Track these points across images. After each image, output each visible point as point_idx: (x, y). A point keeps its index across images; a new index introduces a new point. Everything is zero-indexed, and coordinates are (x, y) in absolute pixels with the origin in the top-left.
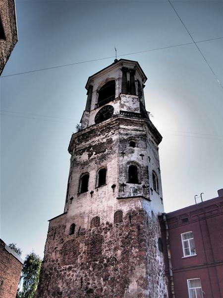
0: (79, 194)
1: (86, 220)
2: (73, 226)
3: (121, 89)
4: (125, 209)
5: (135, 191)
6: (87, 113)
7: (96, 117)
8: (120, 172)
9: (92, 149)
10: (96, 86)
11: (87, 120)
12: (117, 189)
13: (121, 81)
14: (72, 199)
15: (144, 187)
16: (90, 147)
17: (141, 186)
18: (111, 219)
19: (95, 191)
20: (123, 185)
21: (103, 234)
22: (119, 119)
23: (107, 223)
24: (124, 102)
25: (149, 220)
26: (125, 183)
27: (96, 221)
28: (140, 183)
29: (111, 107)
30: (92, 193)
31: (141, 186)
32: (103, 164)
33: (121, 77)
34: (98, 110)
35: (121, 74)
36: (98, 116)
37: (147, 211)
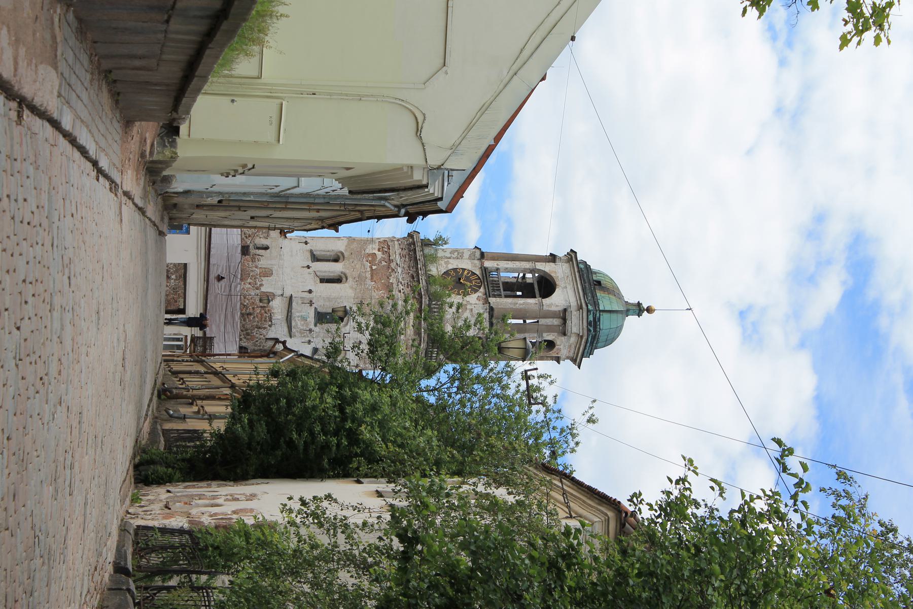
0: (311, 251)
1: (269, 262)
2: (266, 248)
3: (512, 306)
4: (278, 307)
5: (304, 319)
6: (478, 254)
7: (464, 270)
8: (329, 299)
9: (384, 263)
10: (547, 268)
11: (462, 257)
12: (307, 294)
13: (536, 308)
14: (306, 243)
15: (310, 331)
16: (390, 261)
17: (312, 326)
18: (263, 289)
19: (310, 270)
20: (311, 303)
21: (249, 280)
22: (421, 297)
23: (261, 285)
24: (471, 310)
25: (264, 332)
26: (314, 306)
27: (267, 273)
28: (315, 325)
29: (476, 291)
30: (308, 267)
31: (312, 326)
32: (350, 279)
33: (545, 308)
34: (478, 272)
35: (554, 308)
36: (466, 272)
37: (273, 327)
